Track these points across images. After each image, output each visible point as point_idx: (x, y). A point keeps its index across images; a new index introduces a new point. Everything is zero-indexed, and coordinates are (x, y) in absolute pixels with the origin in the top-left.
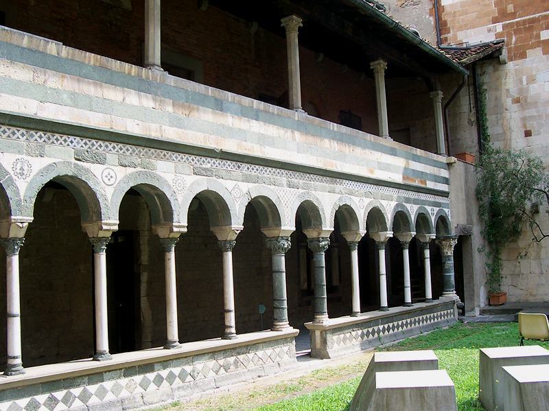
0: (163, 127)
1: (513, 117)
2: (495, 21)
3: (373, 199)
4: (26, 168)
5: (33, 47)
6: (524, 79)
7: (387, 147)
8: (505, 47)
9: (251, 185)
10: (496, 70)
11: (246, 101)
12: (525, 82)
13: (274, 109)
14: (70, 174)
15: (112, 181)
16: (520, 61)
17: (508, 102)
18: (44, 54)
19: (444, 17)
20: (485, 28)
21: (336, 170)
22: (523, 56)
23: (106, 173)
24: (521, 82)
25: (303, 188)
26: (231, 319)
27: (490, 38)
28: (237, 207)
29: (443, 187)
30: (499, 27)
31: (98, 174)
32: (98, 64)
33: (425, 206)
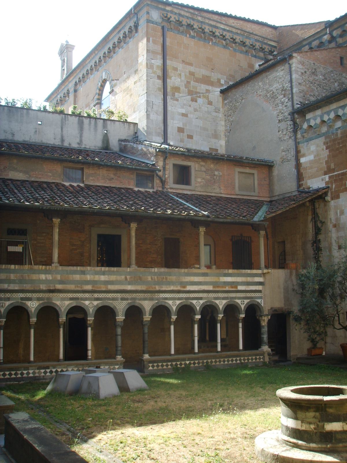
0: (56, 285)
1: (334, 235)
2: (325, 174)
3: (184, 300)
4: (3, 305)
5: (6, 267)
6: (339, 211)
7: (200, 273)
8: (329, 191)
9: (98, 302)
10: (325, 205)
12: (339, 215)
13: (115, 269)
14: (18, 305)
15: (34, 306)
16: (336, 200)
17: (330, 226)
18: (10, 269)
19: (302, 171)
20: (320, 178)
22: (338, 197)
23: (32, 303)
24: (337, 214)
25: (130, 300)
27: (322, 185)
28: (91, 311)
29: (259, 288)
30: (327, 178)
31: (29, 305)
32: (29, 269)
33: (235, 300)
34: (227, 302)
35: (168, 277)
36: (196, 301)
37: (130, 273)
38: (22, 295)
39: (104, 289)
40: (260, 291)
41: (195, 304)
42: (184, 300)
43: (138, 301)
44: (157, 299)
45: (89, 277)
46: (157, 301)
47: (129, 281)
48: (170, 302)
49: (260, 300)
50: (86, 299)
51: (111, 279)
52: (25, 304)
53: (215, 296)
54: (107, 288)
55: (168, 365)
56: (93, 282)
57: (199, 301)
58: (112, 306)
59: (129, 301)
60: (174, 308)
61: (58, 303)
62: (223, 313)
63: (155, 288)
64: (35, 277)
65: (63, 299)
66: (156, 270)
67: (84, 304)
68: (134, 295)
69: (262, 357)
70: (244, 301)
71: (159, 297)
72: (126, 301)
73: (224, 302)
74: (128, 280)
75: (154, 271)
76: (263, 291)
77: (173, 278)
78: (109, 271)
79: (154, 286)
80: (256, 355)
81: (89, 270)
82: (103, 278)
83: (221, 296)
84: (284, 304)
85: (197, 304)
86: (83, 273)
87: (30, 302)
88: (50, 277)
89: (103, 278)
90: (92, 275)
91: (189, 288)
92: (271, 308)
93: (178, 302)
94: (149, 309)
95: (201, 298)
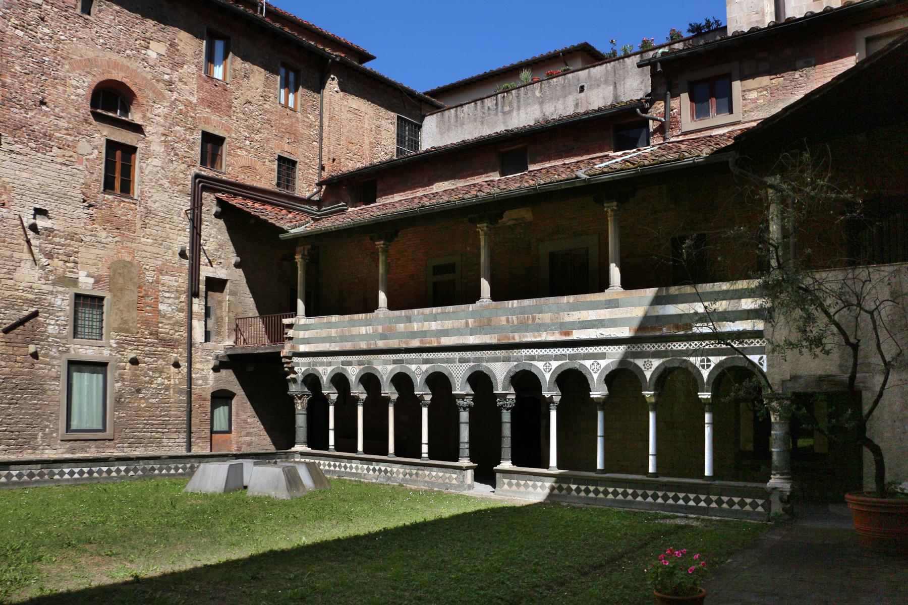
3: (568, 361)
7: (601, 301)
11: (427, 310)
21: (511, 341)
25: (474, 362)
26: (425, 449)
28: (419, 381)
29: (760, 325)
34: (663, 363)
35: (537, 316)
36: (592, 361)
37: (473, 314)
38: (342, 358)
39: (435, 345)
40: (758, 334)
41: (589, 367)
42: (568, 361)
43: (484, 364)
44: (517, 360)
45: (416, 326)
46: (515, 363)
47: (471, 328)
48: (540, 365)
49: (758, 356)
50: (411, 362)
51: (446, 328)
52: (345, 370)
53: (633, 350)
54: (440, 343)
55: (612, 493)
56: (422, 334)
57: (599, 361)
58: (446, 373)
59: (472, 364)
60: (548, 376)
61: (379, 368)
62: (652, 387)
63: (514, 338)
64: (355, 331)
65: (385, 363)
66: (515, 303)
67: (410, 369)
68: (478, 354)
69: (760, 502)
70: (709, 361)
71: (519, 354)
72: (467, 364)
73: (656, 363)
74: (470, 326)
75: (512, 305)
76: (765, 333)
77: (547, 317)
78: (442, 313)
79: (511, 335)
80: (742, 493)
81: (416, 314)
82: (434, 326)
83: (648, 349)
84: (841, 366)
85: (593, 367)
86: (409, 320)
87: (351, 367)
88: (370, 330)
89: (434, 326)
90: (420, 322)
91: (577, 335)
92: (794, 378)
93: (555, 364)
94: (503, 377)
95: (603, 356)
